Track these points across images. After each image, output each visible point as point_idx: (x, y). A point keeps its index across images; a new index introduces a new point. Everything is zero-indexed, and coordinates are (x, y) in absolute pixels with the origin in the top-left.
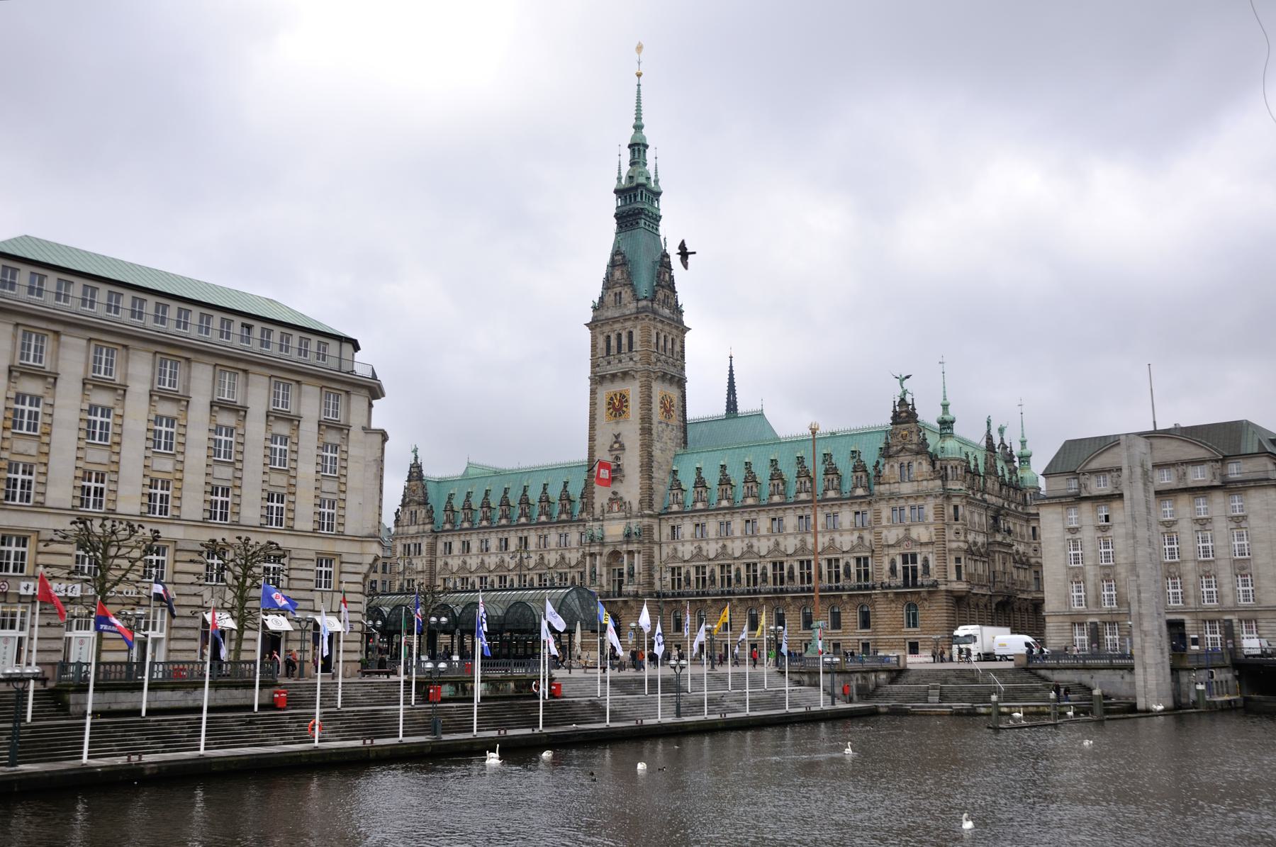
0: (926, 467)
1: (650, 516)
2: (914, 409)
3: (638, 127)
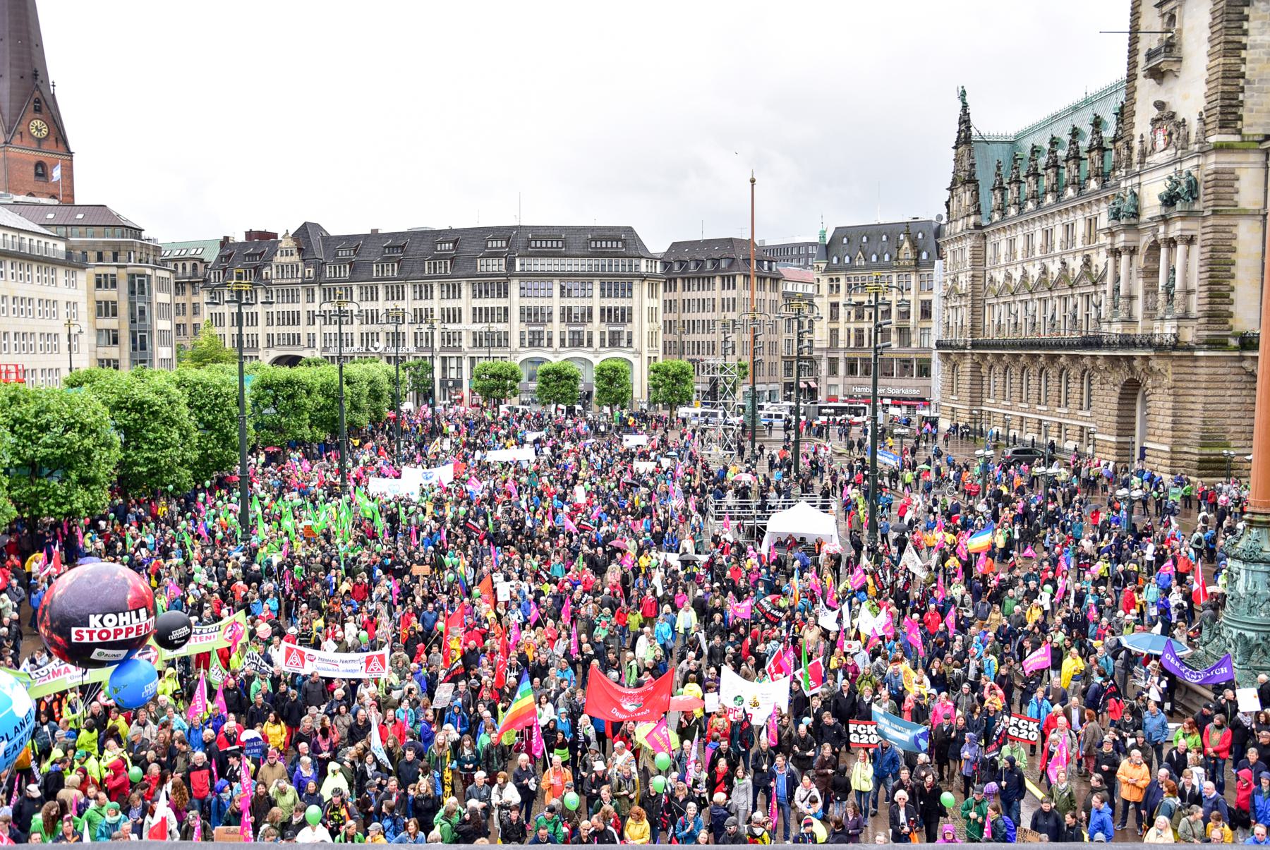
1: (1221, 148)
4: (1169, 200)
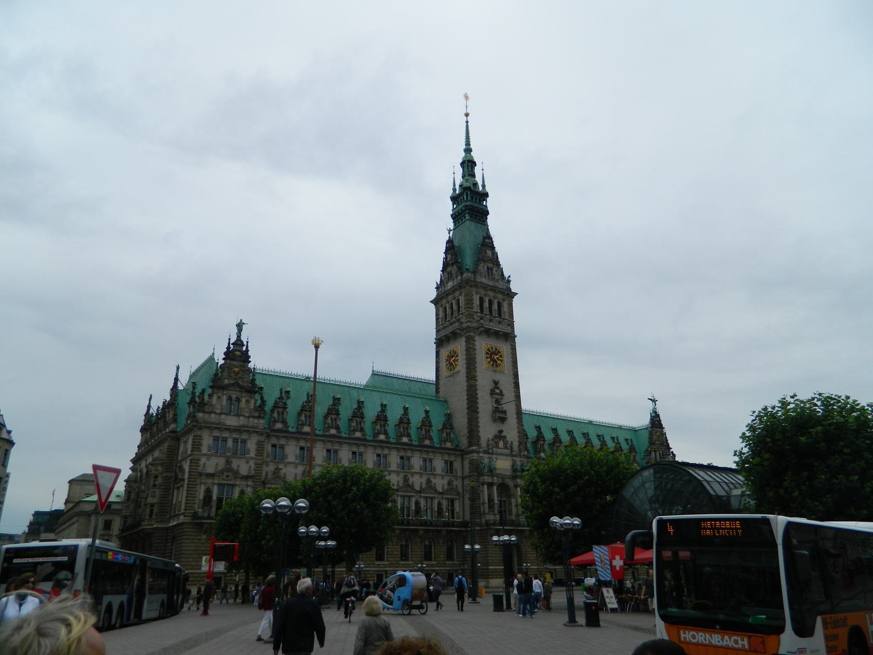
3: (468, 150)
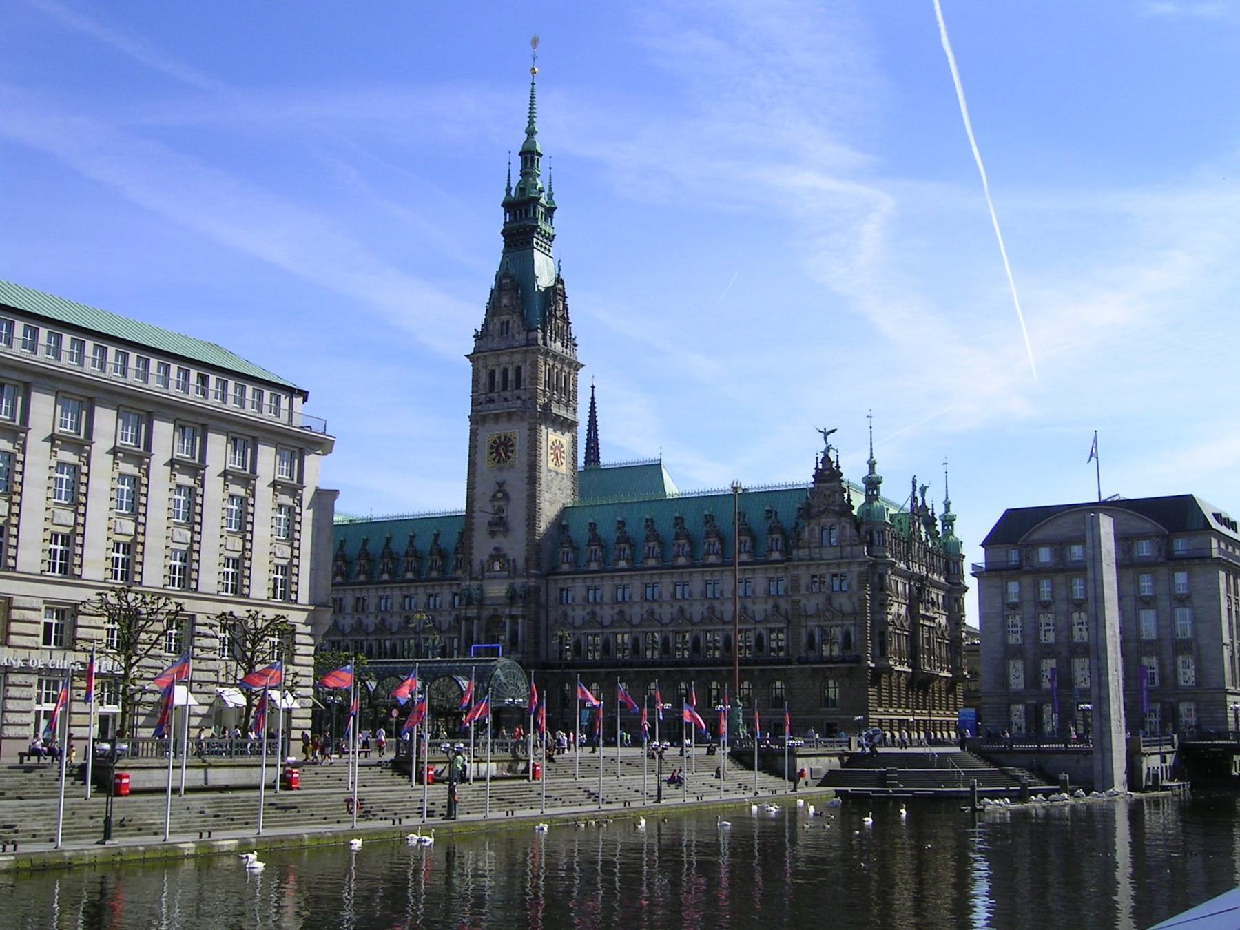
0: (849, 531)
1: (536, 576)
2: (838, 467)
3: (531, 133)
4: (512, 597)
